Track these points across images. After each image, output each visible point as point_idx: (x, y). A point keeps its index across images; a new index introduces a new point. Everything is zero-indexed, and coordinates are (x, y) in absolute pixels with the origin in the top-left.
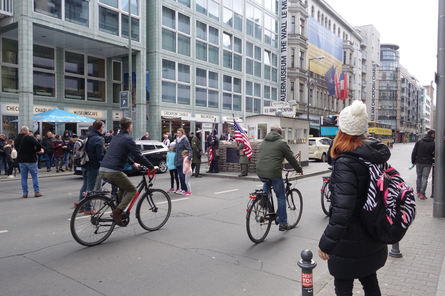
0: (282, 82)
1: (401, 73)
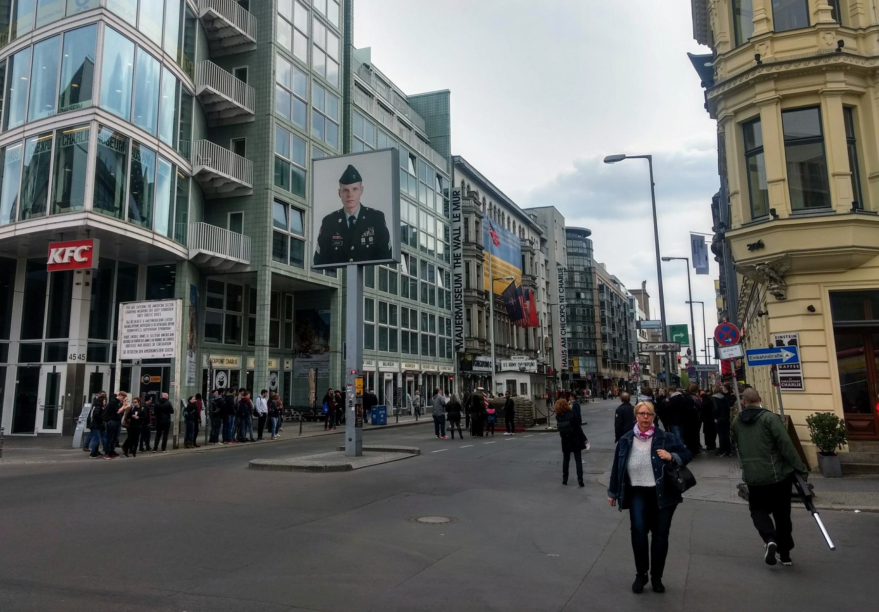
1: (597, 277)
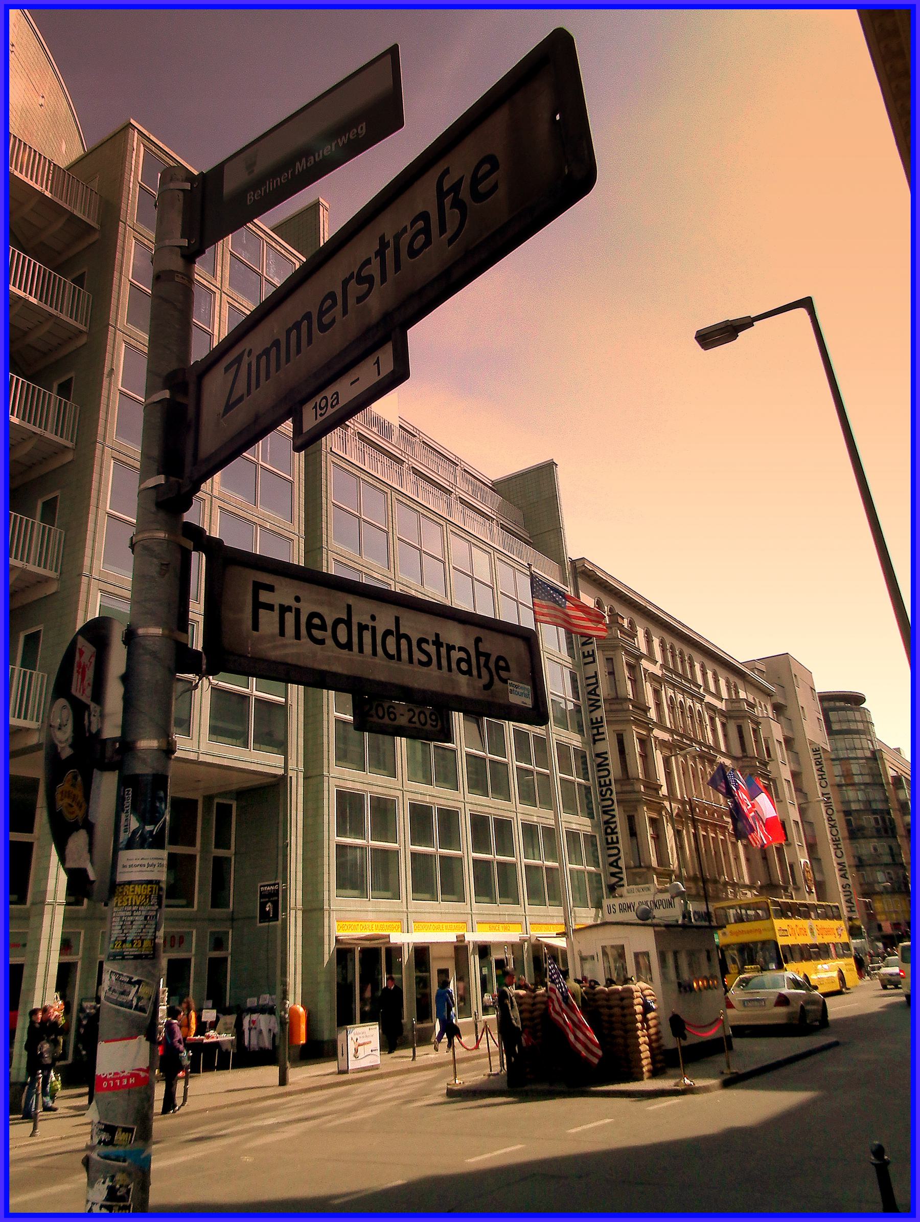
0: (608, 817)
1: (887, 764)
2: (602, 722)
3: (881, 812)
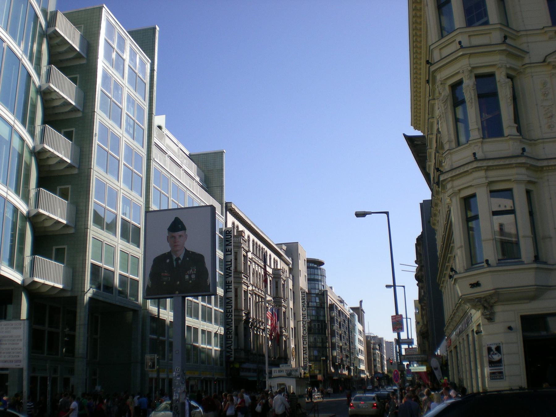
1: (329, 298)
2: (231, 283)
3: (322, 321)
